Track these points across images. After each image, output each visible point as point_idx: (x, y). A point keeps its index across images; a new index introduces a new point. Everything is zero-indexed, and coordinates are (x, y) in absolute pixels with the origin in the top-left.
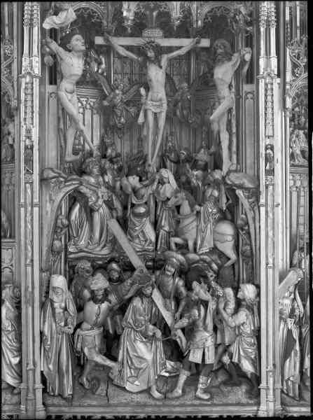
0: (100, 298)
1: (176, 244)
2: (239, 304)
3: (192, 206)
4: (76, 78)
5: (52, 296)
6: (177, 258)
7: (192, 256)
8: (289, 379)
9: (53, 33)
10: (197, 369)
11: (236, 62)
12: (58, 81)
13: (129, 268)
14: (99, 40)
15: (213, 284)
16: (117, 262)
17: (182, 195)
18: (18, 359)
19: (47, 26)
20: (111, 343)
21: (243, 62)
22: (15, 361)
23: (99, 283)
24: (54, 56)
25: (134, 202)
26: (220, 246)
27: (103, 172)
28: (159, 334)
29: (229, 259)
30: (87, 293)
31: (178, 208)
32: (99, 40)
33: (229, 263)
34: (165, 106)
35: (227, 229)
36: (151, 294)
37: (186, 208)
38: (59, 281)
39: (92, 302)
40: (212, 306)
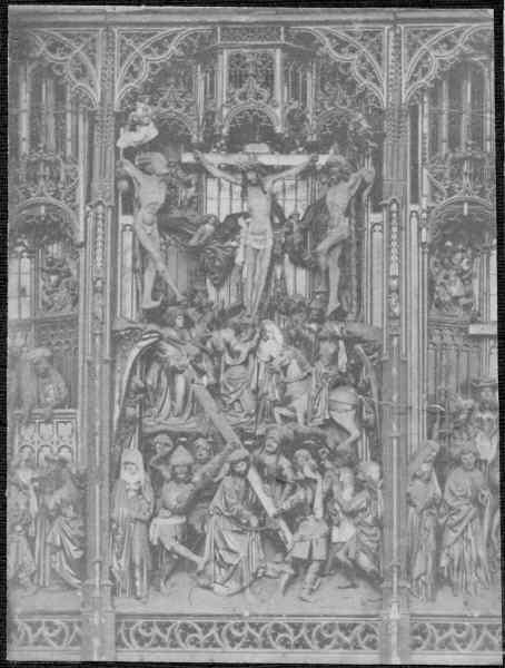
0: (182, 476)
1: (282, 416)
2: (359, 486)
3: (301, 365)
4: (157, 207)
5: (125, 475)
6: (279, 431)
7: (301, 427)
8: (418, 578)
9: (130, 153)
10: (300, 566)
11: (355, 184)
12: (136, 209)
13: (217, 442)
14: (188, 158)
15: (328, 464)
16: (206, 437)
17: (291, 351)
18: (81, 553)
19: (122, 144)
20: (193, 539)
21: (364, 185)
22: (77, 555)
23: (181, 457)
24: (129, 179)
25: (228, 362)
26: (338, 418)
27: (189, 324)
28: (254, 522)
29: (349, 434)
30: (167, 474)
31: (285, 369)
32: (188, 158)
33: (352, 439)
34: (270, 234)
35: (345, 397)
36: (246, 472)
37: (294, 370)
38: (133, 455)
39: (173, 484)
40: (321, 487)
